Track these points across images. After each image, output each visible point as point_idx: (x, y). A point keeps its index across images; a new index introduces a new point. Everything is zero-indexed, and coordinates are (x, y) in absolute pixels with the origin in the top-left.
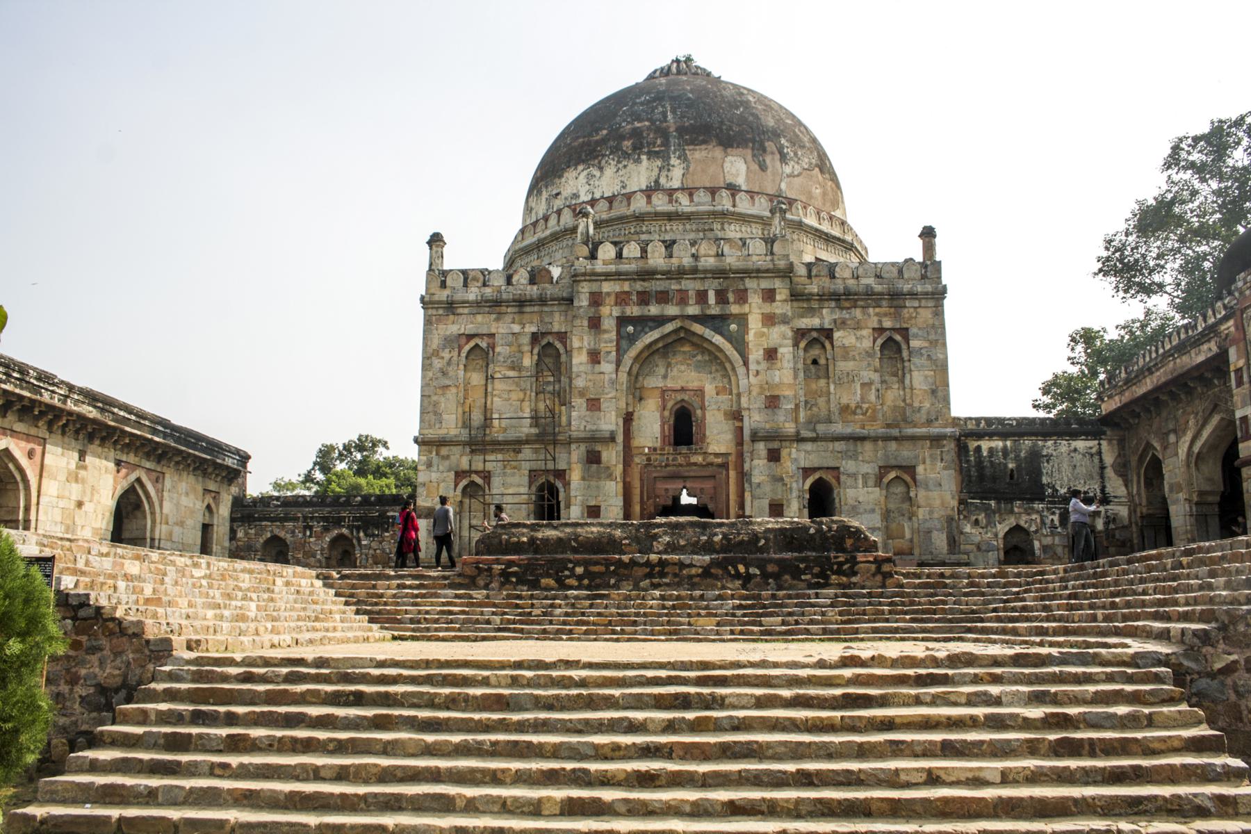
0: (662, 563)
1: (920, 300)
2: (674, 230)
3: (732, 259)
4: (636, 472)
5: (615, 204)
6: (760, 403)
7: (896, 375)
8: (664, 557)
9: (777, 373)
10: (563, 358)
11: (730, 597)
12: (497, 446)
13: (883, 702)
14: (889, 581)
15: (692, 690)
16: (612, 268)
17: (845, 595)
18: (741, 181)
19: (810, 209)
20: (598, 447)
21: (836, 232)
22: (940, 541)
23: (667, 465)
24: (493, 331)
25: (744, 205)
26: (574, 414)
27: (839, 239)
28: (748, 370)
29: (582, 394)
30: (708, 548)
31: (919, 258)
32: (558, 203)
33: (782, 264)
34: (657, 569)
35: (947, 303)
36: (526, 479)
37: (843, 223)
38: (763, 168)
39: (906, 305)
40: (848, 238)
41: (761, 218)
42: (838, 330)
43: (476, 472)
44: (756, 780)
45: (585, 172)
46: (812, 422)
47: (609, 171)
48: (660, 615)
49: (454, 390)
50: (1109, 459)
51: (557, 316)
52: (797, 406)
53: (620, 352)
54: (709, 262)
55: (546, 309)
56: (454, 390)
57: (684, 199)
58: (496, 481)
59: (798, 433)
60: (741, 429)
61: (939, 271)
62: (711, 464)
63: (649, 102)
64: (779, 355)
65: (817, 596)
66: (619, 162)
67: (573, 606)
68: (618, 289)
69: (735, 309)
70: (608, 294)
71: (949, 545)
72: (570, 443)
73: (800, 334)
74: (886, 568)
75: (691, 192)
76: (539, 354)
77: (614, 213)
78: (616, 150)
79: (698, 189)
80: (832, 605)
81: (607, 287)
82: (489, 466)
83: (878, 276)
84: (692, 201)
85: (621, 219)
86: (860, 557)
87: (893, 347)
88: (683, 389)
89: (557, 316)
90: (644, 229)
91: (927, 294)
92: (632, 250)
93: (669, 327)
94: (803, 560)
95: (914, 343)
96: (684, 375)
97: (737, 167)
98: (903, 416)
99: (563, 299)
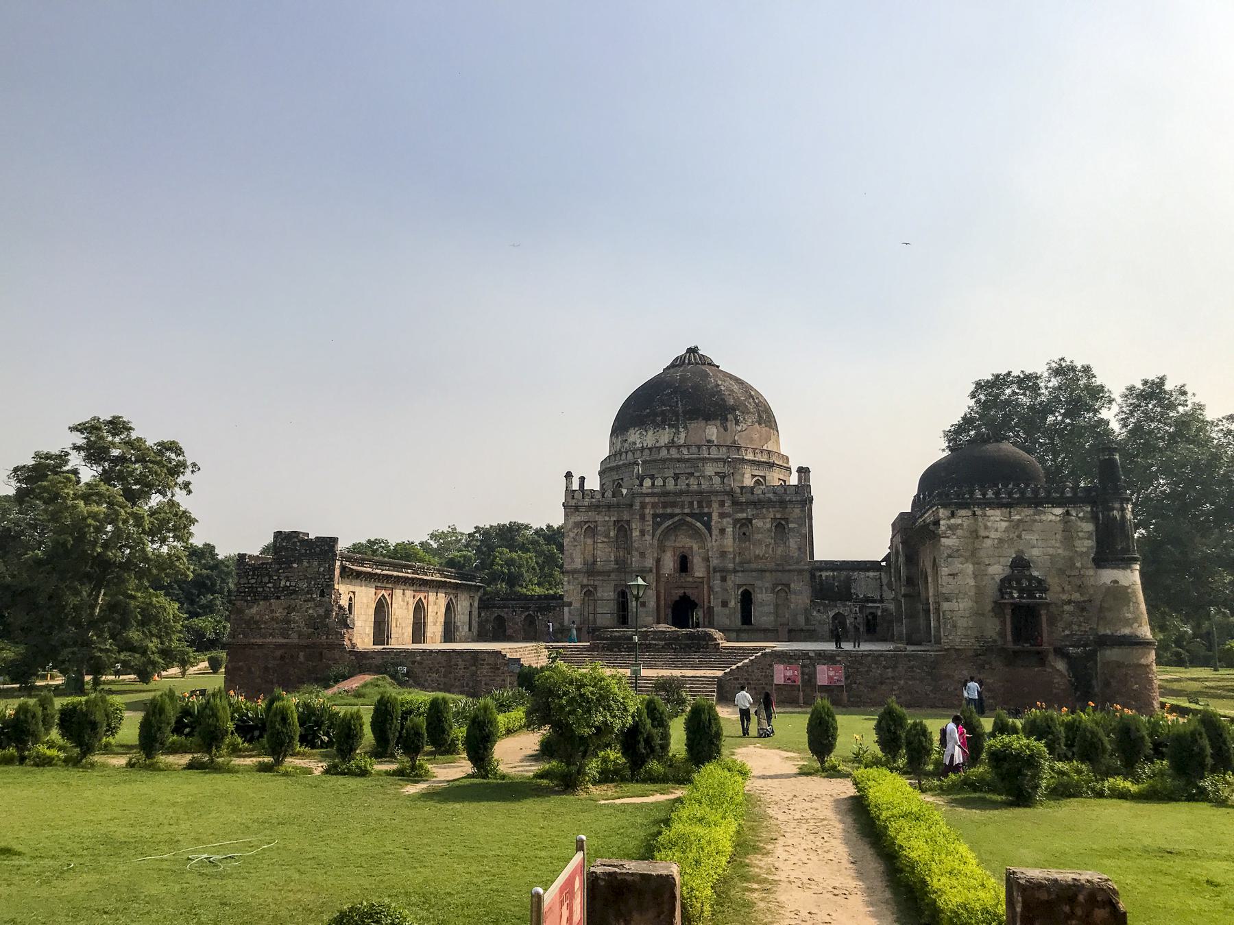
2: (681, 468)
3: (705, 485)
11: (669, 655)
18: (714, 438)
22: (801, 620)
25: (714, 453)
30: (664, 639)
32: (626, 445)
33: (728, 489)
37: (769, 452)
38: (726, 430)
39: (793, 505)
46: (741, 563)
47: (650, 433)
50: (885, 581)
53: (654, 530)
58: (600, 590)
69: (706, 510)
73: (736, 521)
75: (688, 447)
78: (653, 422)
81: (647, 500)
85: (655, 461)
87: (781, 527)
92: (659, 482)
93: (677, 518)
96: (684, 541)
97: (712, 432)
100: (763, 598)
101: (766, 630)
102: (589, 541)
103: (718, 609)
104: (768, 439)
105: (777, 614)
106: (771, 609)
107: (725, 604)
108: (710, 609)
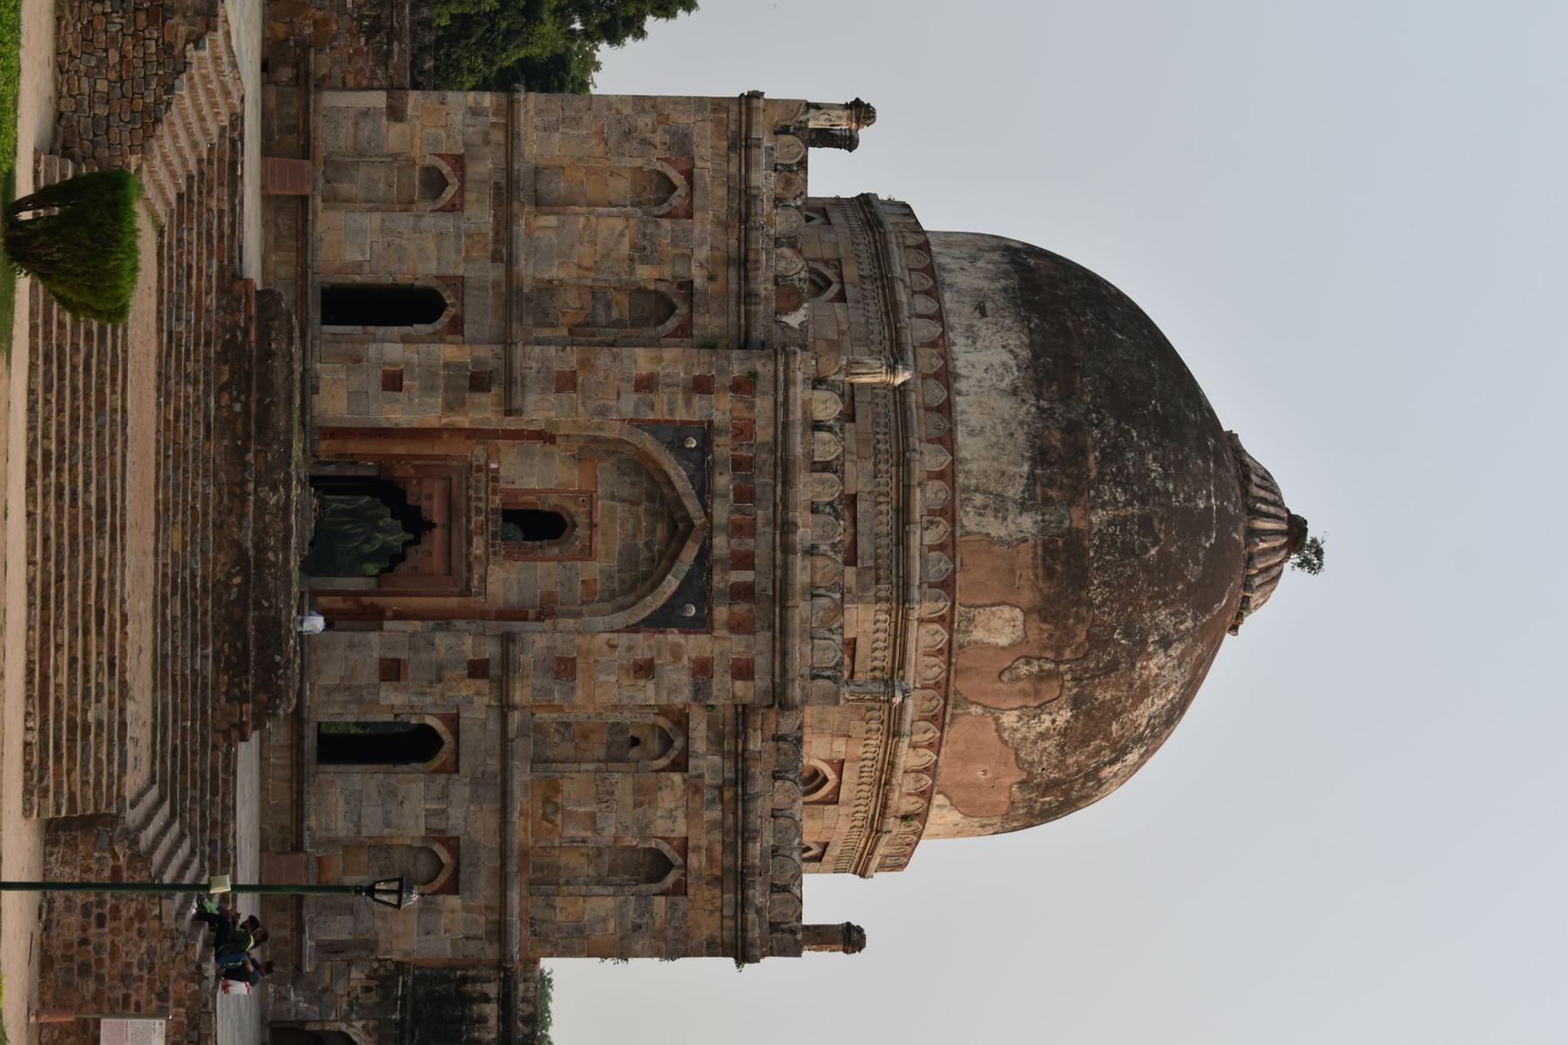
0: (244, 495)
1: (735, 917)
3: (801, 610)
4: (457, 448)
5: (935, 417)
6: (563, 647)
7: (612, 872)
8: (251, 498)
9: (613, 679)
10: (649, 332)
12: (505, 223)
13: (99, 633)
14: (220, 736)
15: (108, 520)
16: (797, 415)
17: (205, 685)
19: (927, 757)
20: (495, 390)
21: (902, 801)
23: (469, 498)
24: (697, 215)
25: (923, 638)
26: (552, 349)
27: (885, 806)
28: (617, 631)
29: (585, 363)
30: (261, 548)
31: (810, 918)
33: (796, 693)
34: (238, 491)
35: (725, 964)
36: (451, 272)
37: (922, 816)
40: (891, 823)
41: (902, 667)
42: (685, 781)
43: (462, 189)
44: (59, 552)
45: (1012, 363)
47: (1005, 406)
48: (185, 493)
49: (599, 151)
51: (722, 321)
52: (560, 709)
53: (654, 427)
54: (801, 573)
55: (732, 304)
56: (599, 151)
57: (932, 536)
58: (448, 222)
59: (514, 708)
60: (525, 619)
61: (783, 953)
62: (470, 570)
63: (1143, 476)
64: (641, 683)
65: (205, 657)
66: (1021, 423)
67: (197, 403)
68: (761, 422)
69: (721, 613)
70: (751, 407)
71: (331, 943)
72: (504, 343)
74: (235, 734)
75: (947, 547)
76: (656, 292)
77: (915, 414)
79: (953, 559)
80: (193, 670)
81: (763, 404)
82: (471, 210)
83: (775, 851)
84: (931, 548)
85: (904, 429)
86: (248, 707)
87: (654, 866)
88: (592, 526)
89: (722, 321)
90: (883, 467)
91: (744, 929)
93: (692, 506)
94: (246, 646)
95: (660, 904)
96: (615, 528)
98: (545, 879)
99: (747, 333)
100: (407, 805)
101: (298, 808)
102: (621, 187)
103: (375, 644)
104: (967, 808)
105: (351, 847)
106: (372, 826)
107: (391, 671)
108: (371, 617)
